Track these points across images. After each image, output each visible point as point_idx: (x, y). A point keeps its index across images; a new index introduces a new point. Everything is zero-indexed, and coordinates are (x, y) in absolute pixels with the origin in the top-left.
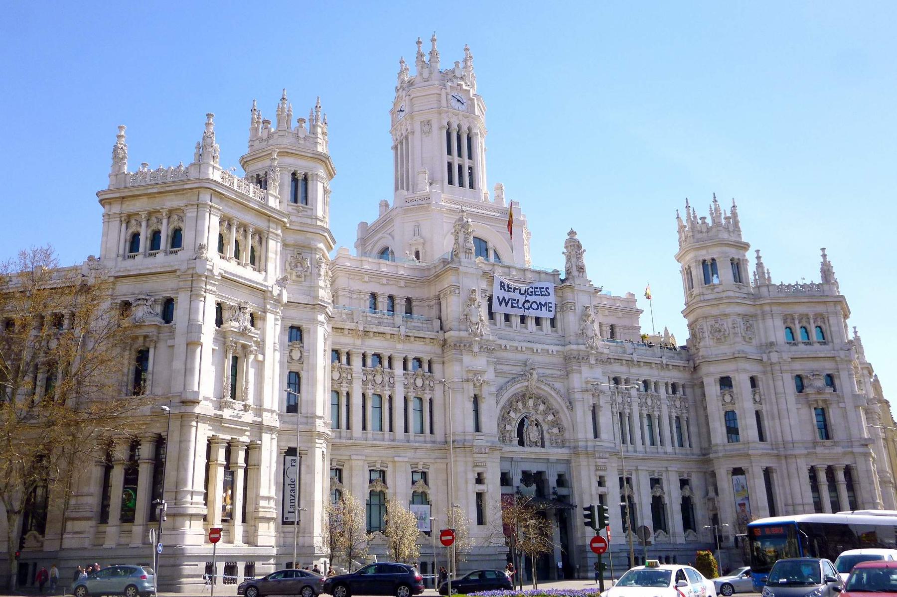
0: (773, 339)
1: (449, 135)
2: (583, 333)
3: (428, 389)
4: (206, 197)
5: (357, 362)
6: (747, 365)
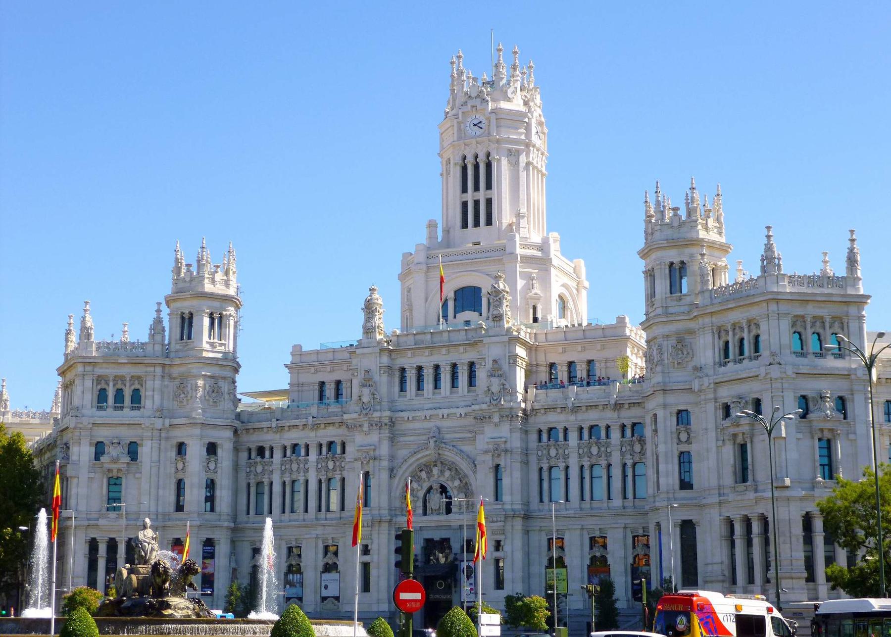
0: (702, 361)
1: (464, 169)
2: (489, 390)
3: (338, 469)
4: (80, 369)
5: (278, 454)
6: (671, 399)
